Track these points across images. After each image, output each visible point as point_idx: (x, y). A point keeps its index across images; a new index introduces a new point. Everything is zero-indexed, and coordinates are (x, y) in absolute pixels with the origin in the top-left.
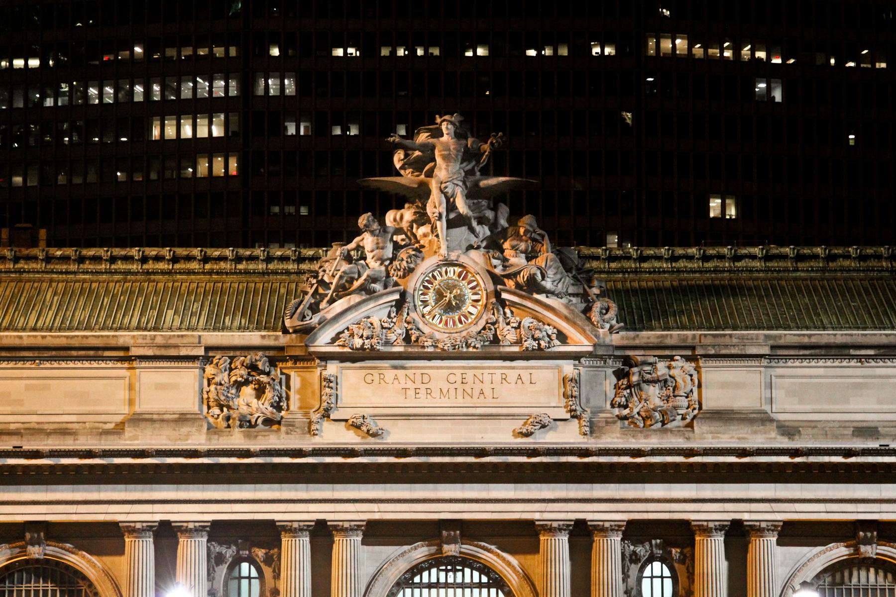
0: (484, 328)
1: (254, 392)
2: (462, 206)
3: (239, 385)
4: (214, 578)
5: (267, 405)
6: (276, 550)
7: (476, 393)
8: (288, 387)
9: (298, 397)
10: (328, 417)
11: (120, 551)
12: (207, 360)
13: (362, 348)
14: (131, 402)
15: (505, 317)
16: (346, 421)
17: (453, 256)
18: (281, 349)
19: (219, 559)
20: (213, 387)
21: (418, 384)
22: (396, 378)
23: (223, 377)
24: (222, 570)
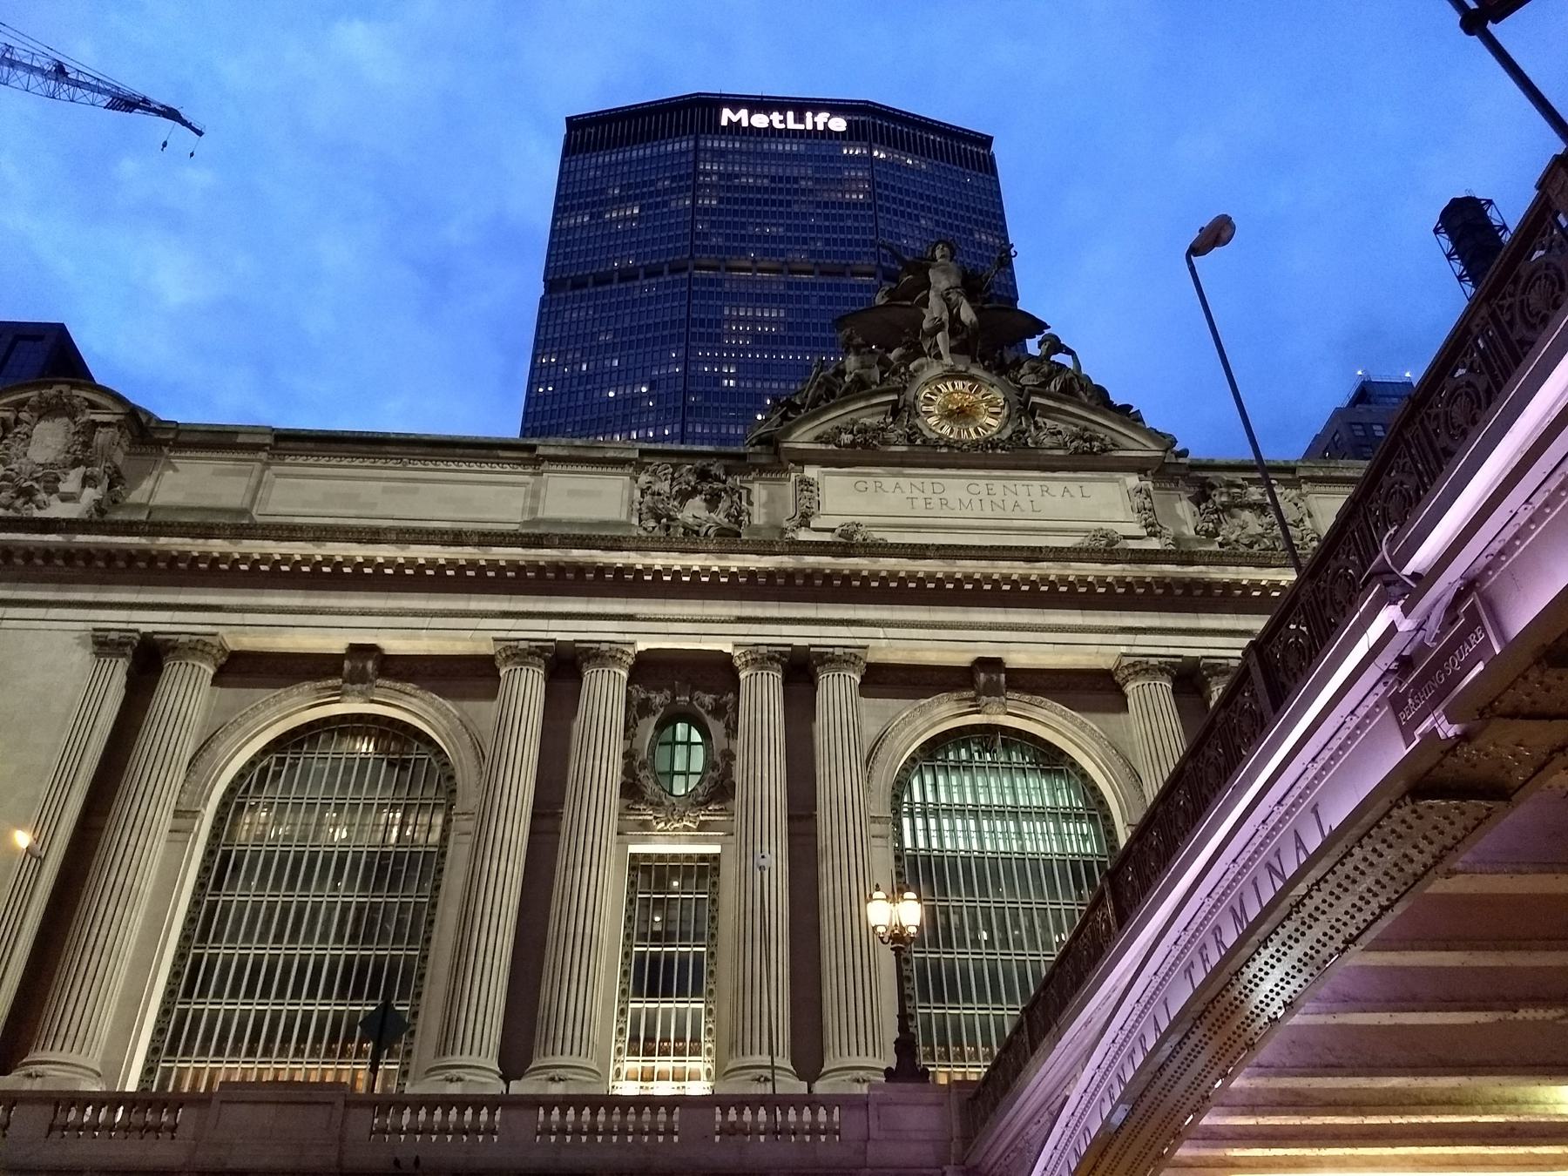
0: (1010, 438)
1: (704, 504)
2: (967, 314)
3: (685, 496)
4: (634, 735)
5: (722, 516)
6: (731, 696)
7: (1009, 504)
8: (750, 503)
9: (763, 510)
10: (808, 526)
11: (492, 695)
12: (640, 466)
13: (853, 444)
14: (533, 510)
15: (1038, 428)
16: (833, 530)
17: (961, 367)
18: (742, 457)
19: (644, 709)
20: (648, 498)
21: (928, 493)
22: (897, 486)
23: (664, 487)
24: (648, 727)
